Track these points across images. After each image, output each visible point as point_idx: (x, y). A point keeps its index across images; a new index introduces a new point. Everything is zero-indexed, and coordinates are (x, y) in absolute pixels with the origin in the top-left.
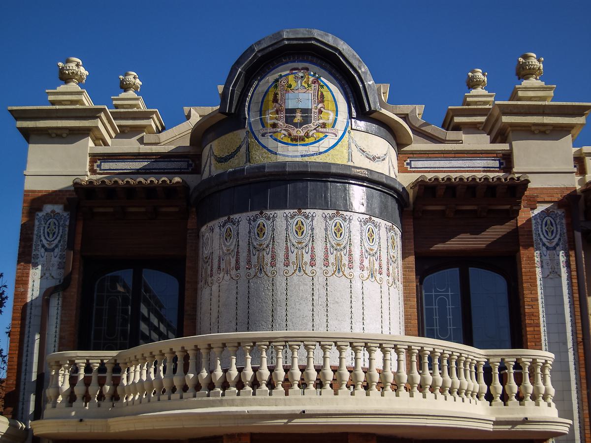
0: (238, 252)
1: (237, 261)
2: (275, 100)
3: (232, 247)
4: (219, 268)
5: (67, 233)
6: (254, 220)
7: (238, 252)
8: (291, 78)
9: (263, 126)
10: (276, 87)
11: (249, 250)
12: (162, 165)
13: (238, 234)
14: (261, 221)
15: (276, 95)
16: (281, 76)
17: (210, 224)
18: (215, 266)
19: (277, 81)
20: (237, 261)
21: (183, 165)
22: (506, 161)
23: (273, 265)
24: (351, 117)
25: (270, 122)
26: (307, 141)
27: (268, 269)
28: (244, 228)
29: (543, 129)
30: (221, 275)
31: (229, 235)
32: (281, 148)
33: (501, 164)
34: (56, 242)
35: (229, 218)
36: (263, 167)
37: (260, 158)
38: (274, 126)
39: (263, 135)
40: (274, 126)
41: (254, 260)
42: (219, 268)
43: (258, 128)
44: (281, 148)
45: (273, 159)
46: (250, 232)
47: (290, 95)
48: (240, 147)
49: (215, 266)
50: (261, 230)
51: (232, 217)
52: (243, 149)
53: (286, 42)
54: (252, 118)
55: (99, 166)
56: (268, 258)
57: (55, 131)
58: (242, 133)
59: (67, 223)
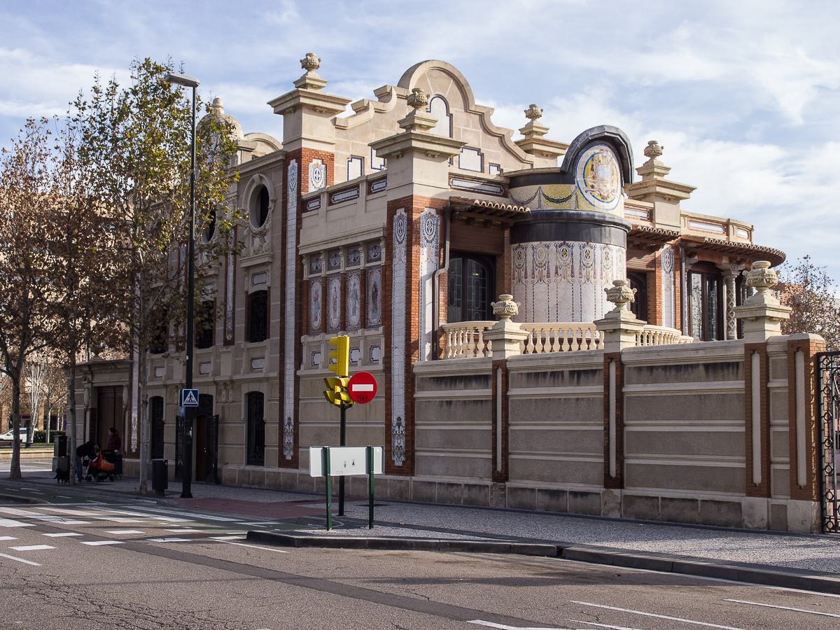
0: (572, 266)
1: (572, 272)
2: (592, 170)
3: (568, 262)
4: (557, 273)
5: (439, 230)
6: (583, 248)
7: (572, 266)
8: (600, 155)
9: (586, 186)
10: (593, 160)
11: (581, 266)
12: (487, 188)
13: (572, 254)
14: (587, 248)
15: (593, 165)
16: (595, 154)
17: (548, 243)
18: (552, 271)
19: (593, 156)
20: (572, 272)
21: (498, 189)
22: (651, 215)
23: (595, 278)
24: (622, 186)
25: (591, 184)
26: (609, 200)
27: (592, 279)
28: (576, 250)
29: (670, 197)
30: (558, 278)
31: (564, 253)
32: (596, 203)
33: (648, 216)
34: (433, 236)
35: (564, 243)
36: (594, 216)
37: (585, 209)
38: (592, 187)
39: (586, 192)
40: (592, 187)
41: (584, 272)
42: (557, 273)
43: (582, 186)
44: (596, 203)
45: (591, 208)
46: (580, 254)
47: (599, 168)
48: (571, 196)
49: (552, 271)
50: (588, 256)
51: (567, 242)
52: (574, 198)
53: (606, 134)
54: (579, 178)
55: (452, 182)
56: (592, 273)
57: (432, 153)
58: (573, 187)
59: (439, 224)
